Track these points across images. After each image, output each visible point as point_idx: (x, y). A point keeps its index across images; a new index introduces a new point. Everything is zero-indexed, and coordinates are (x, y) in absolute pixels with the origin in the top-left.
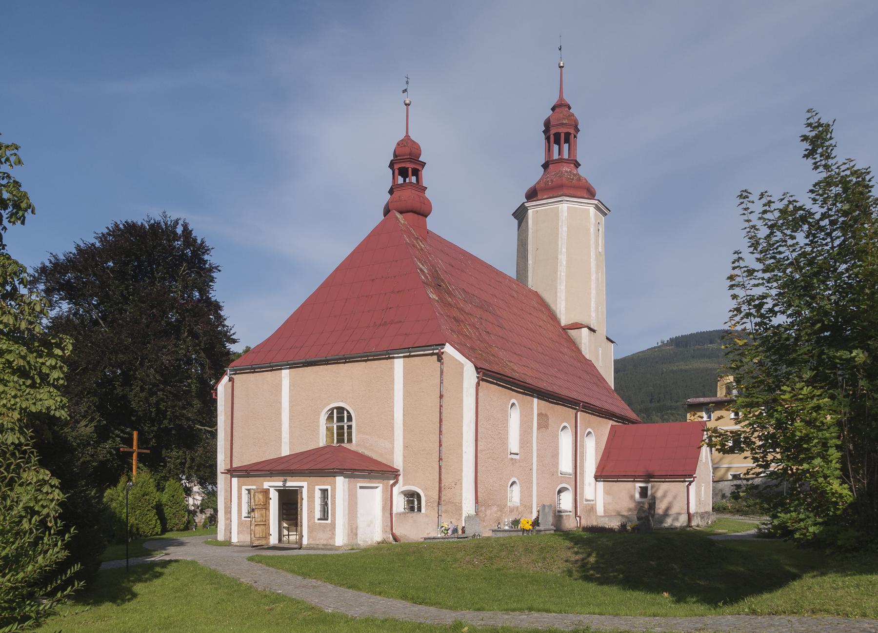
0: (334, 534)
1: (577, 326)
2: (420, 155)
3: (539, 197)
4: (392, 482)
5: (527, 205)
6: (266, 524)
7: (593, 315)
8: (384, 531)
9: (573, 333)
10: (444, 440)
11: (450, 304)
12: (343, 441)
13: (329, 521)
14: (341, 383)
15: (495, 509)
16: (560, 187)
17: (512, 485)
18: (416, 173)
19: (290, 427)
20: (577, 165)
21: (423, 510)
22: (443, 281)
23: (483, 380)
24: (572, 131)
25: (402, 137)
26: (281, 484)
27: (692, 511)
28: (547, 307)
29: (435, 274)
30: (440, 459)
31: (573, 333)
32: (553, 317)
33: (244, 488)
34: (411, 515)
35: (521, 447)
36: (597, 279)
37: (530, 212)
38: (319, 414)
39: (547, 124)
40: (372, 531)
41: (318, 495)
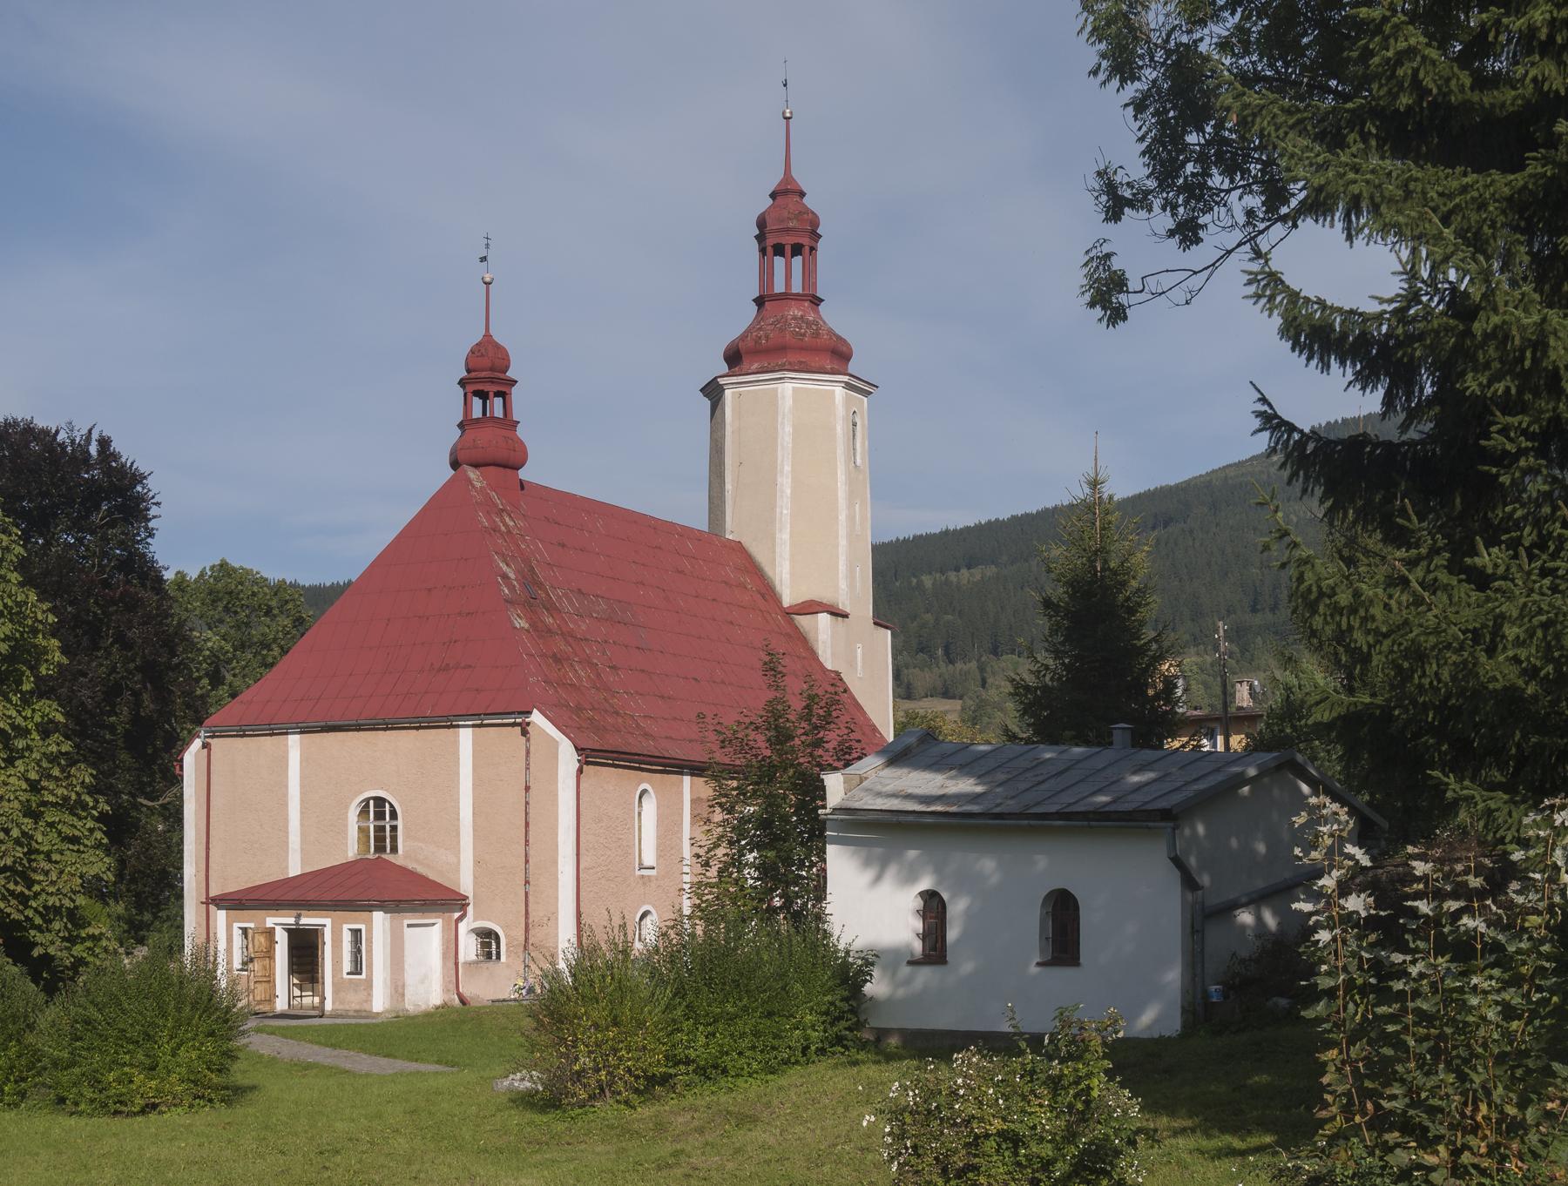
0: (370, 995)
1: (812, 608)
2: (507, 367)
3: (745, 366)
4: (457, 915)
5: (721, 381)
6: (270, 981)
8: (446, 990)
9: (803, 621)
10: (531, 852)
11: (549, 631)
12: (383, 849)
13: (363, 976)
14: (382, 760)
16: (782, 349)
17: (642, 918)
19: (302, 825)
20: (816, 301)
21: (503, 958)
22: (541, 586)
23: (588, 763)
24: (805, 241)
25: (478, 338)
26: (292, 920)
28: (753, 569)
29: (530, 579)
30: (527, 882)
31: (803, 621)
32: (767, 591)
33: (236, 925)
35: (659, 857)
36: (851, 518)
37: (728, 393)
38: (347, 807)
39: (761, 223)
40: (427, 989)
41: (347, 937)
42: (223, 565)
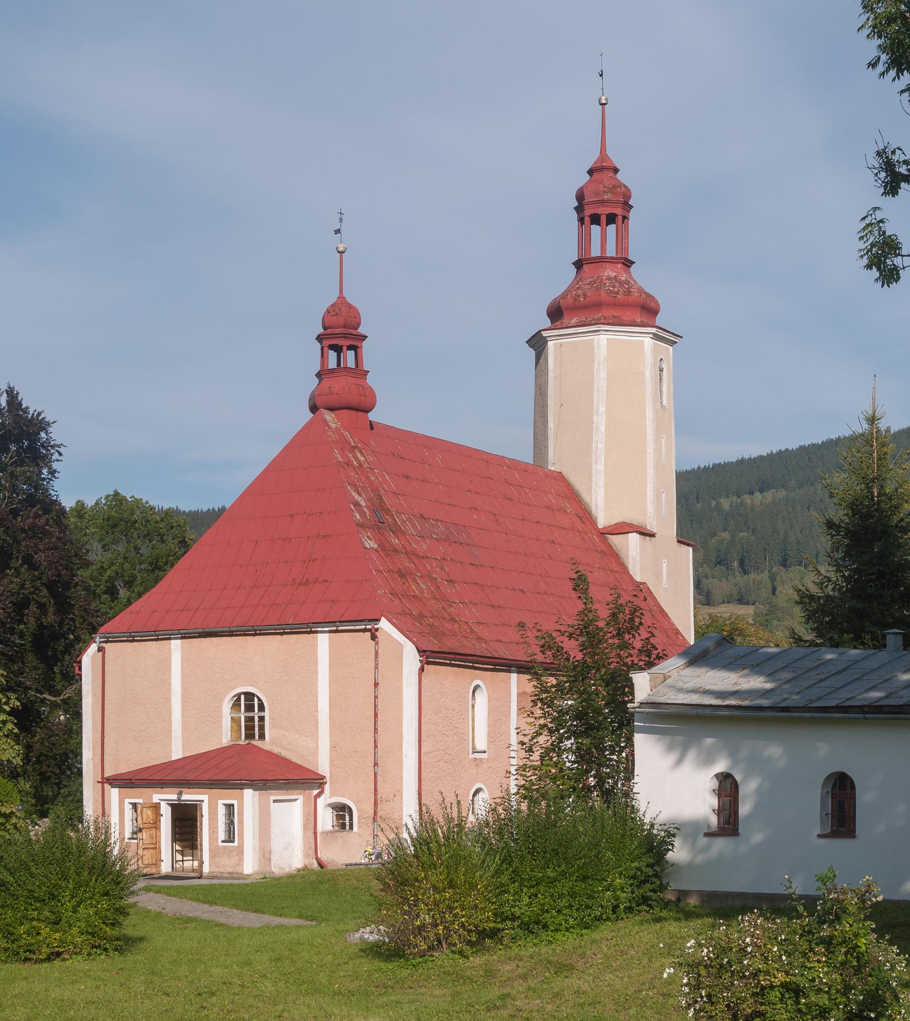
19: (183, 716)
38: (221, 701)
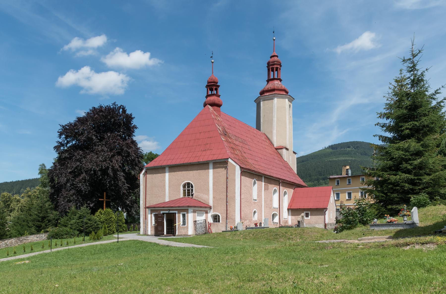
7: (288, 143)
9: (279, 151)
15: (248, 221)
18: (216, 89)
21: (221, 222)
24: (279, 66)
27: (327, 222)
34: (216, 223)
35: (258, 197)
36: (289, 128)
39: (268, 63)
42: (151, 152)
